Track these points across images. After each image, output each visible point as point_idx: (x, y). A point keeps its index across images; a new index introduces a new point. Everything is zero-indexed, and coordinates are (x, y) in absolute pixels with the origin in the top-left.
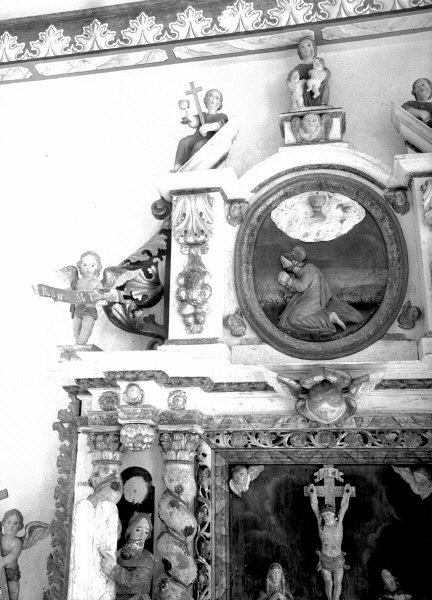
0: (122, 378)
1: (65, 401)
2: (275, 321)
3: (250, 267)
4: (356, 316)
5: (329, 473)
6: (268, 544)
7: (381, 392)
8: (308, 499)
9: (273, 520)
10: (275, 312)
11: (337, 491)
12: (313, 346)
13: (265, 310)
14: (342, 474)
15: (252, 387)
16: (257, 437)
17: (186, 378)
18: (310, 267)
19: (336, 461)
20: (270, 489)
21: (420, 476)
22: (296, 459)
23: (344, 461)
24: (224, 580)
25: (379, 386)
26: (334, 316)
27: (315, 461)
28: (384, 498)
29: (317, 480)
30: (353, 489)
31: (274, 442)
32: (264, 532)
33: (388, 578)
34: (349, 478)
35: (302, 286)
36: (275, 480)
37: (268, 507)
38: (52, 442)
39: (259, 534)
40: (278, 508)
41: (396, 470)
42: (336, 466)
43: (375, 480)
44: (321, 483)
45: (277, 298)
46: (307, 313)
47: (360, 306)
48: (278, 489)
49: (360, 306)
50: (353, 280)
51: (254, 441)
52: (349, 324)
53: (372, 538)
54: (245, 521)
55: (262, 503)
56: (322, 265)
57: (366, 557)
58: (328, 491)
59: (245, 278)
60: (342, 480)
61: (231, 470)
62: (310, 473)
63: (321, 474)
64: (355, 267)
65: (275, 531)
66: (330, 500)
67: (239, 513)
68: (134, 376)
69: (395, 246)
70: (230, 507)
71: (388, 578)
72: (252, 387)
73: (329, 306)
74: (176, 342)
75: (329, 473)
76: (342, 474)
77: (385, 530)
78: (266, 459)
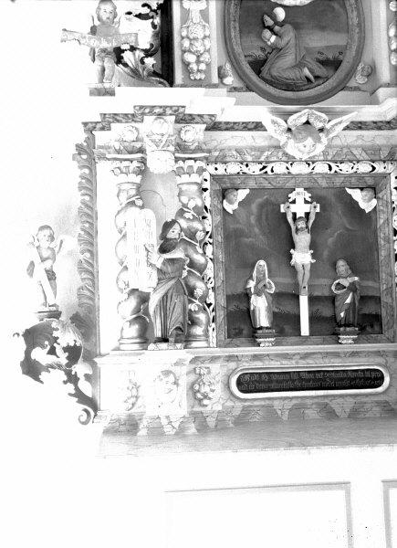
0: (151, 113)
1: (81, 137)
2: (258, 73)
3: (237, 25)
4: (321, 71)
5: (300, 195)
6: (252, 247)
7: (347, 132)
8: (285, 214)
9: (257, 230)
10: (258, 66)
11: (307, 208)
12: (289, 94)
13: (250, 63)
14: (310, 195)
15: (246, 127)
16: (247, 165)
17: (199, 115)
18: (288, 27)
19: (306, 185)
20: (254, 207)
21: (368, 193)
22: (274, 184)
23: (310, 185)
24: (221, 274)
25: (347, 128)
26: (306, 72)
27: (289, 185)
28: (340, 212)
29: (290, 200)
30: (318, 205)
31: (261, 170)
32: (250, 239)
33: (342, 265)
34: (316, 198)
35: (282, 43)
36: (259, 200)
37: (253, 219)
38: (74, 172)
39: (248, 240)
40: (259, 219)
41: (349, 191)
42: (305, 189)
43: (333, 200)
44: (294, 202)
45: (259, 54)
46: (283, 66)
47: (324, 63)
48: (261, 206)
49: (324, 63)
50: (319, 41)
51: (245, 170)
52: (317, 77)
53: (330, 241)
54: (235, 230)
55: (248, 217)
56: (297, 27)
57: (326, 253)
58: (300, 208)
59: (233, 34)
60: (309, 200)
61: (224, 194)
62: (285, 194)
63: (292, 196)
64: (323, 28)
65: (258, 237)
66: (300, 214)
67: (232, 226)
68: (161, 110)
69: (355, 13)
70: (224, 224)
71: (342, 265)
72: (246, 127)
73: (299, 65)
74: (178, 86)
75: (300, 195)
76: (310, 195)
77: (340, 235)
78: (252, 184)
